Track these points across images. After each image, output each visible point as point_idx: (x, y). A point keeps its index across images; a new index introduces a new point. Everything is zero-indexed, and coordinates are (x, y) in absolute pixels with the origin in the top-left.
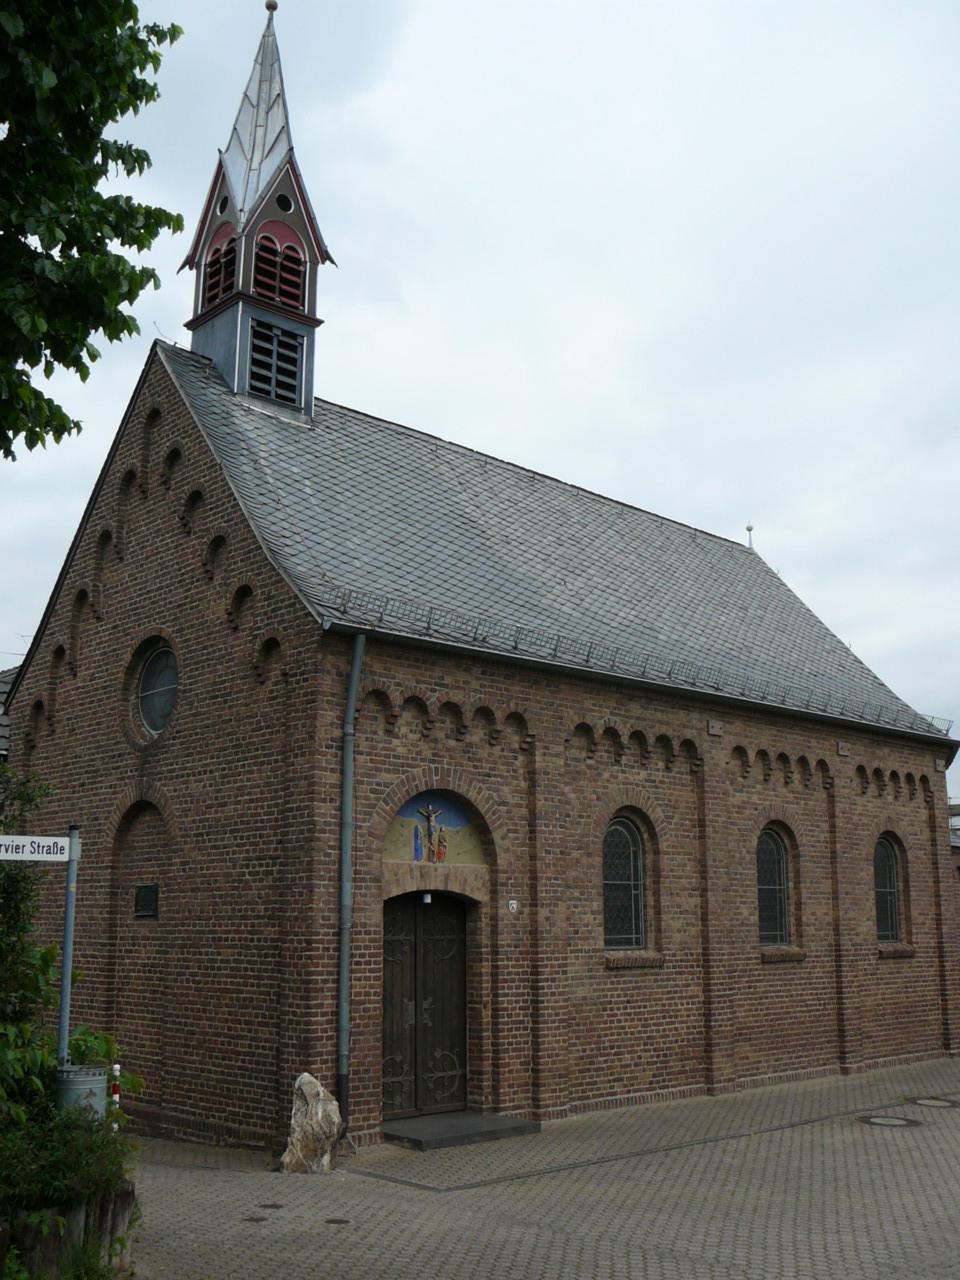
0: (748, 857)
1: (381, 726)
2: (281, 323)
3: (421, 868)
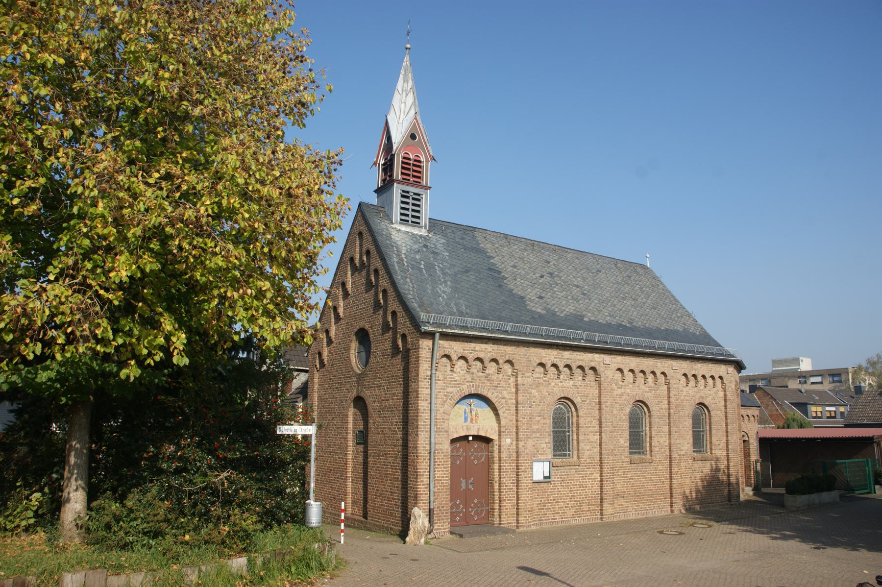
0: (624, 418)
1: (449, 368)
2: (412, 190)
3: (467, 426)
